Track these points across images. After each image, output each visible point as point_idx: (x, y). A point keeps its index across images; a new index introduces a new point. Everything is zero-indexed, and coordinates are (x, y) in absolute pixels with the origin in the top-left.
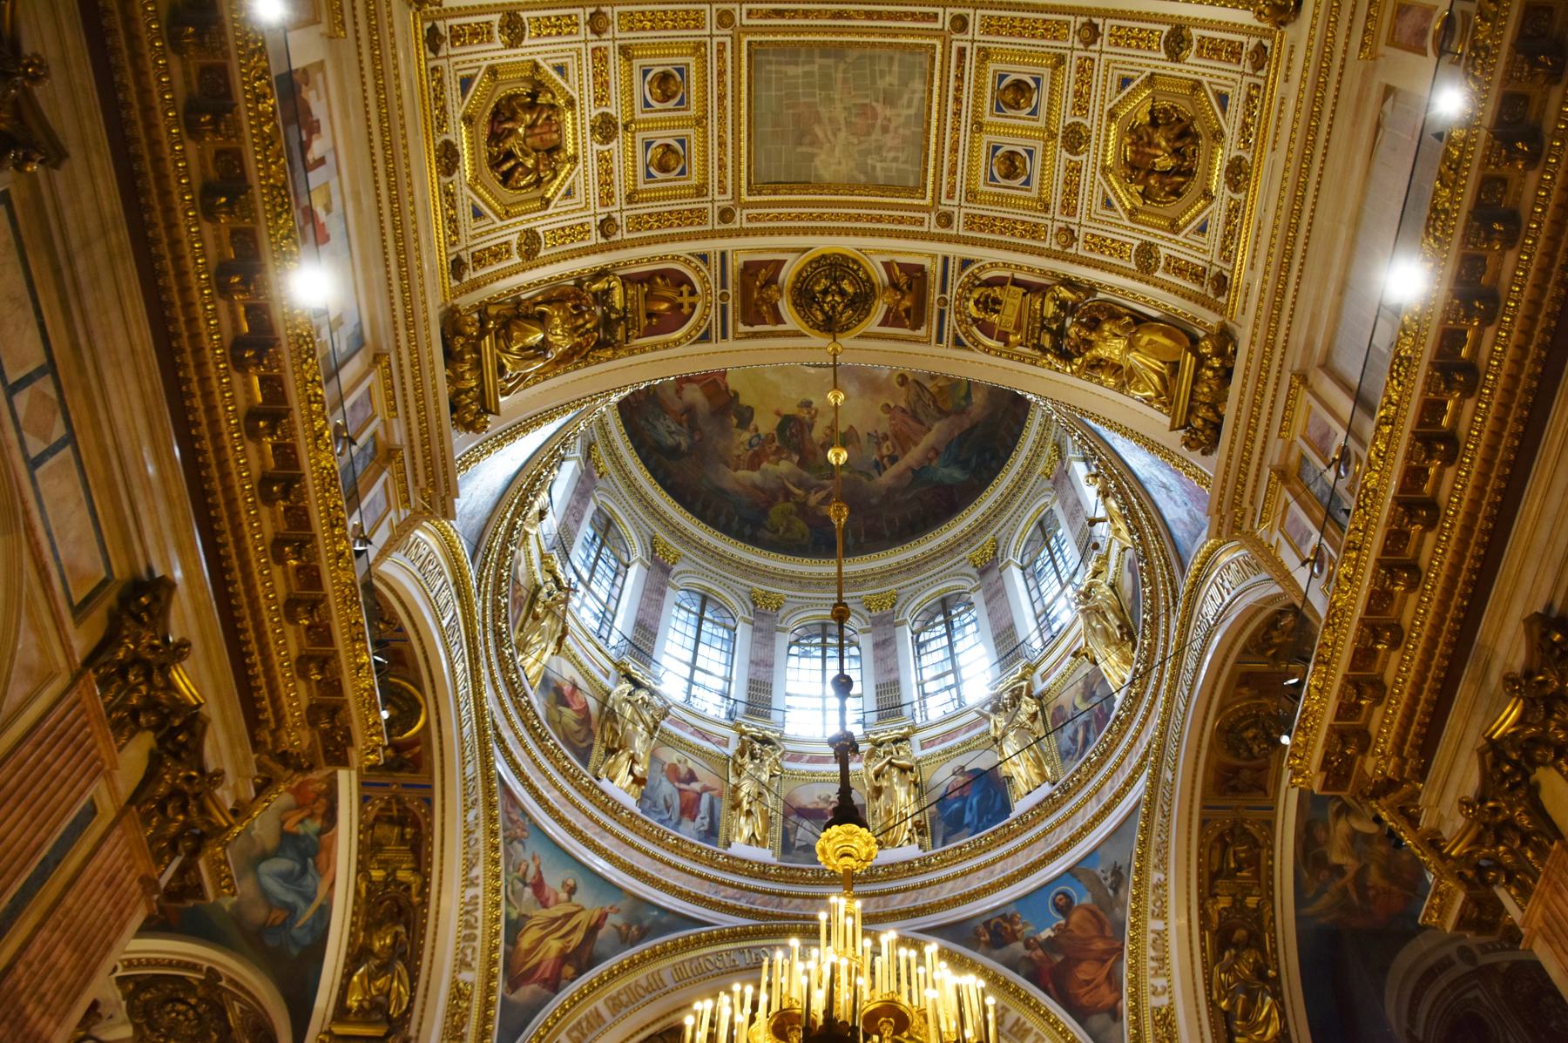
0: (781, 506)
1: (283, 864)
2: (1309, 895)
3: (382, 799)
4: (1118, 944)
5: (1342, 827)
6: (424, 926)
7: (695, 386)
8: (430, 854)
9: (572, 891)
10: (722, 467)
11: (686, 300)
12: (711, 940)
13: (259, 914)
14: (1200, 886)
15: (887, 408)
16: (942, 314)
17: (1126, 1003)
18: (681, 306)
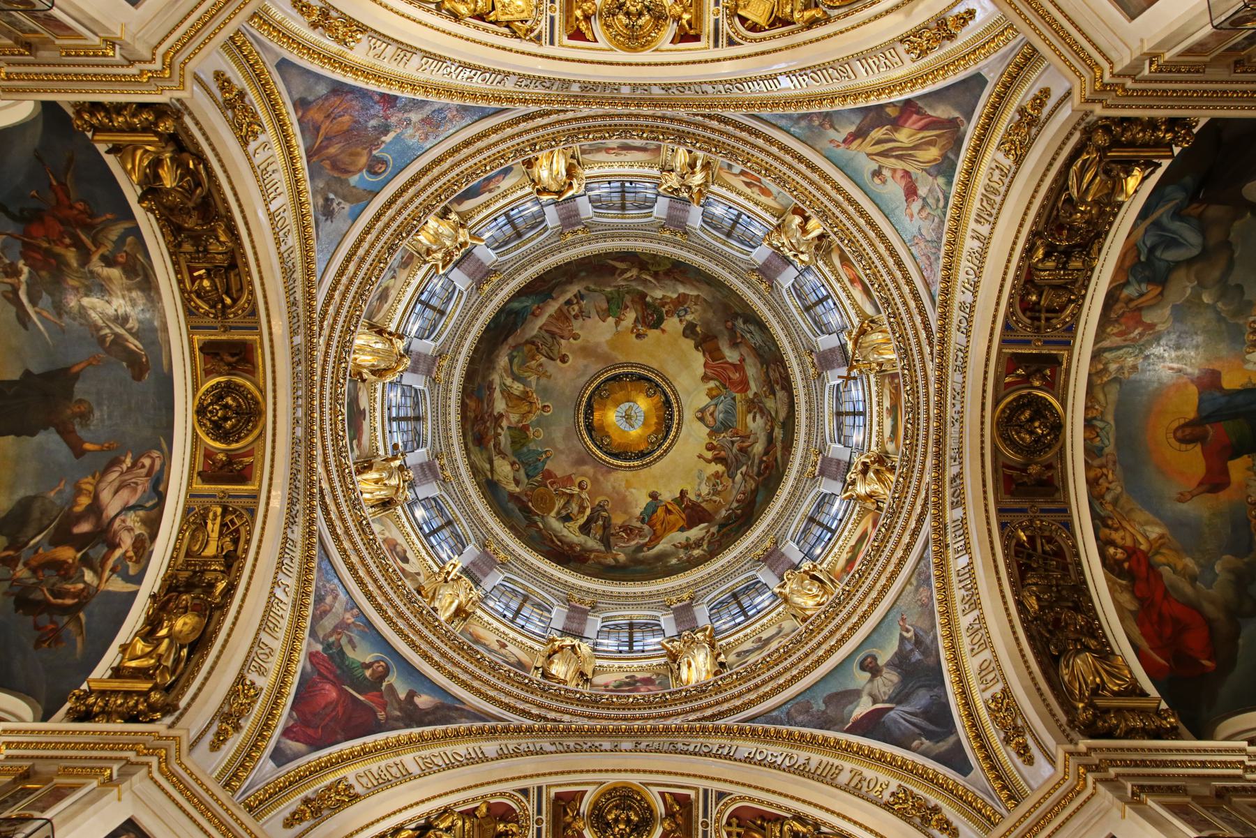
0: (661, 269)
1: (1171, 255)
2: (130, 239)
3: (1055, 329)
4: (315, 159)
5: (119, 304)
6: (1039, 215)
8: (1016, 277)
9: (877, 173)
10: (709, 299)
11: (735, 829)
13: (1214, 211)
14: (244, 255)
15: (576, 337)
16: (539, 812)
17: (292, 118)
18: (738, 826)
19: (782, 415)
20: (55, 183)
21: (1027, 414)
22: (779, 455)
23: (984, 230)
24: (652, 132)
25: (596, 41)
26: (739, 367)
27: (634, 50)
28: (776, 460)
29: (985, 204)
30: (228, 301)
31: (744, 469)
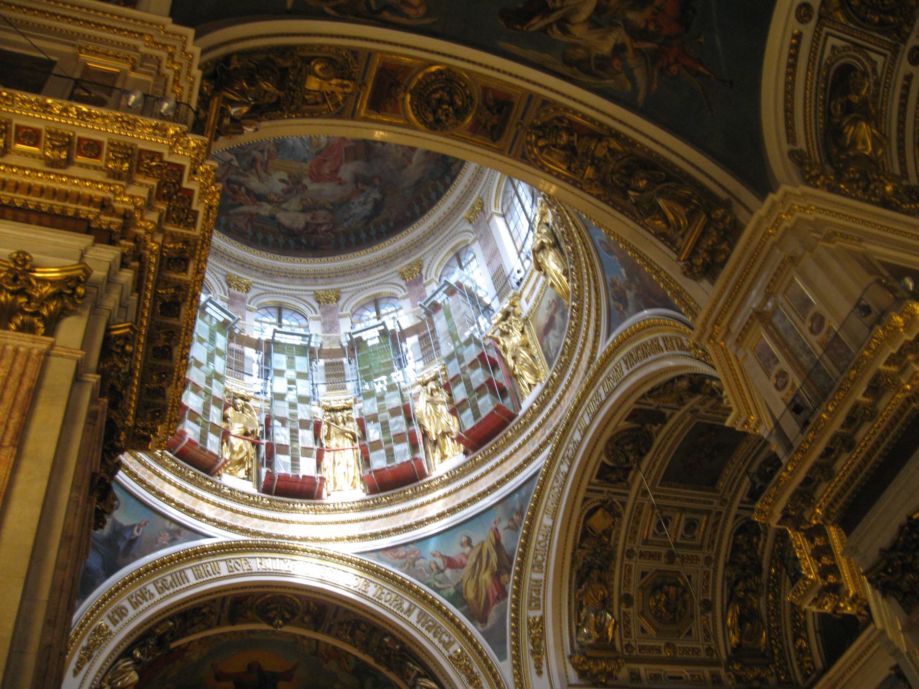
2: (629, 86)
5: (579, 31)
7: (342, 168)
9: (469, 542)
12: (546, 476)
19: (283, 218)
20: (701, 69)
21: (288, 616)
22: (245, 209)
23: (413, 618)
24: (553, 387)
25: (627, 420)
26: (334, 176)
27: (610, 440)
28: (241, 205)
29: (430, 623)
30: (541, 143)
31: (235, 163)
